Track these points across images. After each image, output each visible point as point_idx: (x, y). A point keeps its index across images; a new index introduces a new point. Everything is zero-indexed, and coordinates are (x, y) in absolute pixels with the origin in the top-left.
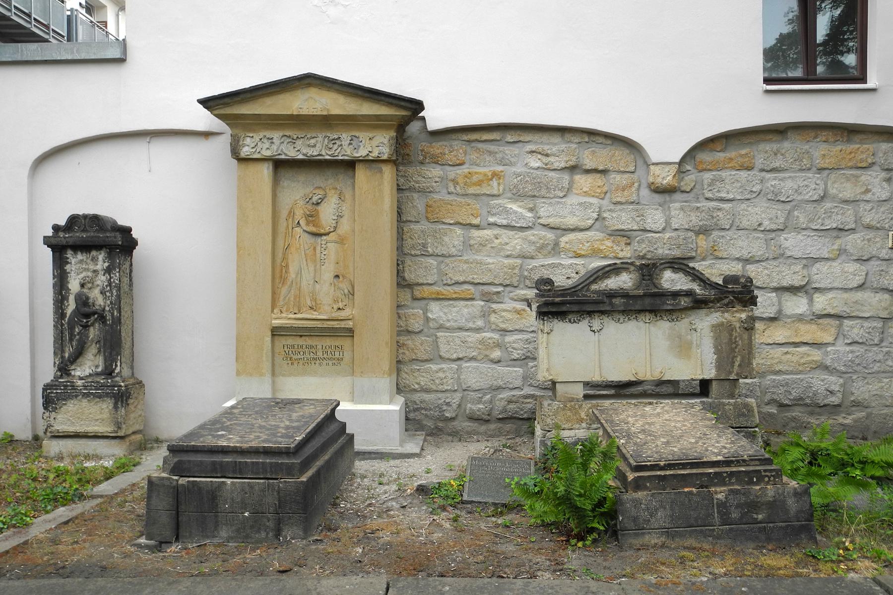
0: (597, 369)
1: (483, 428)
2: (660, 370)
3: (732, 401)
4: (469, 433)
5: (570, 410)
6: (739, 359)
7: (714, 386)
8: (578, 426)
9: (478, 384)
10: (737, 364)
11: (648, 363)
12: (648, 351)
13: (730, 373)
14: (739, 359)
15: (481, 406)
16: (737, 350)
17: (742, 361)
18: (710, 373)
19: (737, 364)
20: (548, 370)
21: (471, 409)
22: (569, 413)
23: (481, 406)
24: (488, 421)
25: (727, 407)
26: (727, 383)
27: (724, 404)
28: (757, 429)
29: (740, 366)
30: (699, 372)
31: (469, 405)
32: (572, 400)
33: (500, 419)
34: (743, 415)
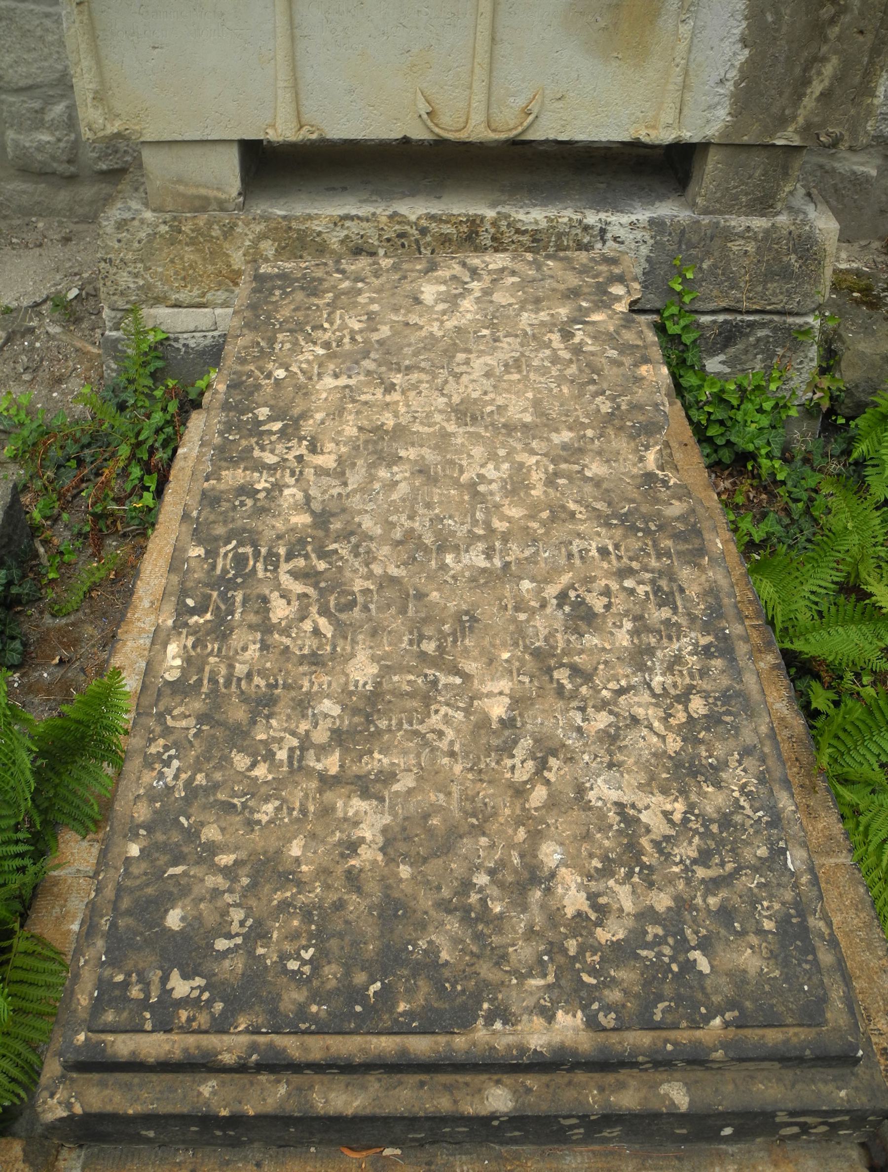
0: (285, 97)
1: (63, 197)
2: (521, 102)
3: (759, 223)
4: (26, 212)
5: (193, 242)
6: (828, 70)
7: (712, 167)
8: (221, 296)
9: (23, 69)
10: (817, 88)
11: (480, 73)
12: (484, 24)
13: (782, 121)
14: (828, 70)
15: (45, 137)
16: (834, 32)
17: (839, 78)
18: (704, 117)
19: (817, 88)
20: (99, 97)
21: (16, 143)
22: (189, 255)
23: (45, 137)
24: (71, 178)
25: (735, 246)
26: (758, 159)
27: (728, 235)
28: (810, 320)
29: (826, 96)
30: (668, 116)
31: (11, 134)
32: (201, 205)
33: (102, 173)
34: (786, 274)
